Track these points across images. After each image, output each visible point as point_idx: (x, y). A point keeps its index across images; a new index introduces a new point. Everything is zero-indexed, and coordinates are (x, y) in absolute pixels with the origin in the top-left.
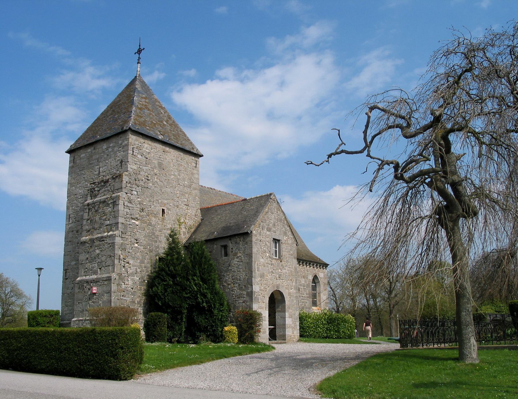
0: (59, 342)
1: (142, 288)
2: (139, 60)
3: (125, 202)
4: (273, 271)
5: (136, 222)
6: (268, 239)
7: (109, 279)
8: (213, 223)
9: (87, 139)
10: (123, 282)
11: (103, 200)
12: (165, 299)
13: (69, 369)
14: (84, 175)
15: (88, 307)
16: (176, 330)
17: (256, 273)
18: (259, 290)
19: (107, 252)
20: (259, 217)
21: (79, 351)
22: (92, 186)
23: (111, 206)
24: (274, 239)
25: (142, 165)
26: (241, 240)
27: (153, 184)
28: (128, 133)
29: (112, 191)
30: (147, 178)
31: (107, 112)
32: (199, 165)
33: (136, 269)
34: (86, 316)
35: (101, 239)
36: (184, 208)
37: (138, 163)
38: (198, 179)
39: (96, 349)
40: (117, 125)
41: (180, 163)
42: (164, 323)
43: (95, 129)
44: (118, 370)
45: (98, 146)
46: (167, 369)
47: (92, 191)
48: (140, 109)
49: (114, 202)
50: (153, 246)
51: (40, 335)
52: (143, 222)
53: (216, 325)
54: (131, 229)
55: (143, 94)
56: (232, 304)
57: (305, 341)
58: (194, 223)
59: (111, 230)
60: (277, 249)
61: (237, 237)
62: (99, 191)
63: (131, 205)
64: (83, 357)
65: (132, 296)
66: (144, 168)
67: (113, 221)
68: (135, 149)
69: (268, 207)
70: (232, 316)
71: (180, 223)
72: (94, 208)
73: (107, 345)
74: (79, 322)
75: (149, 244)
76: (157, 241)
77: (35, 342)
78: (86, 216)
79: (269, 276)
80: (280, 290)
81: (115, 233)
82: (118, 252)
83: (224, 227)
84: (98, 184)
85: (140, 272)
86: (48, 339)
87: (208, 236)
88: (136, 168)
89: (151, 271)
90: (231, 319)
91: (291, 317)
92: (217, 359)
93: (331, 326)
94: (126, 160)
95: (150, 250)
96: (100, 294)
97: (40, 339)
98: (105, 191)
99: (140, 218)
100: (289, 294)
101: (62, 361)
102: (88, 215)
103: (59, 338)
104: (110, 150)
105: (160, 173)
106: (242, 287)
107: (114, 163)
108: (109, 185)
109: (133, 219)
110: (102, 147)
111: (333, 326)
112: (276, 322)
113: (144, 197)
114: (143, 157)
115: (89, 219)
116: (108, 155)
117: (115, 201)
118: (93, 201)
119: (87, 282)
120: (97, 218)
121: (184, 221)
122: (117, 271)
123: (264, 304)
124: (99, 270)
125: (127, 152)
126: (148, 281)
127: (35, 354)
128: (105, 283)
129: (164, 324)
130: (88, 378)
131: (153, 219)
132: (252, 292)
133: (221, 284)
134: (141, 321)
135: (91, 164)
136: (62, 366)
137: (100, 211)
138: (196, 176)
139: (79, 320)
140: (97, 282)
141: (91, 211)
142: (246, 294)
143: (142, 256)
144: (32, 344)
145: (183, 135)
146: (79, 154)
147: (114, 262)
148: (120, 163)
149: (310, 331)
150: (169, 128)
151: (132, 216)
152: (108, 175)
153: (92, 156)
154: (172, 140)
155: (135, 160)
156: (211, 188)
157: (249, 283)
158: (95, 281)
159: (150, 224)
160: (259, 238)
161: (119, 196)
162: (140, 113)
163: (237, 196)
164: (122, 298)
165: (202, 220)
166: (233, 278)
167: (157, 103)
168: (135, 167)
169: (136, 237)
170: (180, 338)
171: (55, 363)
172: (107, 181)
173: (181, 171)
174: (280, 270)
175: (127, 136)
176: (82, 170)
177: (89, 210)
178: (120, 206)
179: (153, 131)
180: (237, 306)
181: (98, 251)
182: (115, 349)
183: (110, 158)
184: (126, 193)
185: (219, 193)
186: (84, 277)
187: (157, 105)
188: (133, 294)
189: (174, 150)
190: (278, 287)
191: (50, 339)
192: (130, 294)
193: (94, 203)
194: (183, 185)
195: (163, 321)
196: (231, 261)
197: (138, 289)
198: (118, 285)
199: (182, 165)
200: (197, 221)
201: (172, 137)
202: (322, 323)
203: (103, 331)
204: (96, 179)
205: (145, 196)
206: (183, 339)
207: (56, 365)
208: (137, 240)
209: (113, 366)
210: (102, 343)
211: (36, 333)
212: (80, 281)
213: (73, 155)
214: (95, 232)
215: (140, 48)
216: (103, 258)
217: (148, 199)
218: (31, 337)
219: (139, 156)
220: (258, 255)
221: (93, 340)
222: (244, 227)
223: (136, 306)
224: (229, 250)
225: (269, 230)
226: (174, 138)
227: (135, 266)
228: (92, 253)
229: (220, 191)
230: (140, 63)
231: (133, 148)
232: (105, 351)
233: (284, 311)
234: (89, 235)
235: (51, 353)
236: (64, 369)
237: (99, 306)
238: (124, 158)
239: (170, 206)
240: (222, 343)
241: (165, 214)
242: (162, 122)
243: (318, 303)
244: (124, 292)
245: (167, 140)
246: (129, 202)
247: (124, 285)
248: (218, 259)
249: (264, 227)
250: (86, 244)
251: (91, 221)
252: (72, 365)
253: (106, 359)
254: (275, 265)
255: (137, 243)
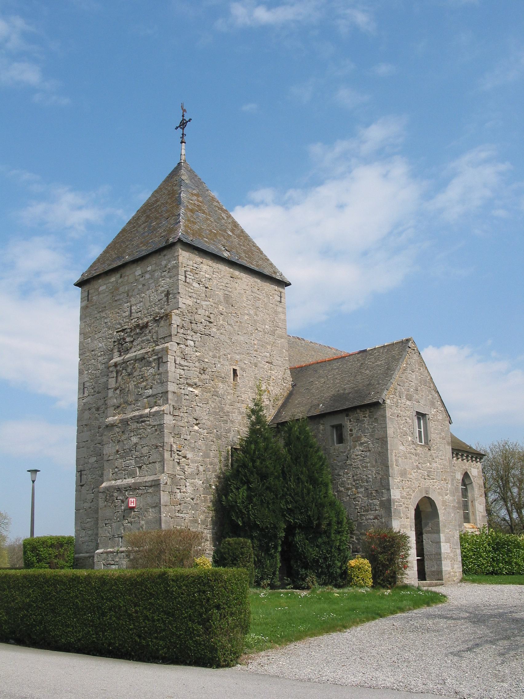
0: (98, 595)
1: (208, 498)
2: (182, 138)
3: (176, 358)
4: (419, 465)
5: (194, 390)
6: (408, 413)
7: (156, 484)
8: (314, 391)
9: (107, 262)
10: (179, 489)
11: (140, 356)
12: (249, 514)
13: (120, 645)
14: (106, 318)
15: (122, 531)
16: (266, 566)
17: (395, 470)
18: (399, 497)
19: (150, 439)
20: (394, 376)
21: (136, 612)
22: (120, 336)
23: (154, 365)
24: (418, 413)
25: (200, 298)
26: (367, 415)
27: (218, 330)
28: (176, 247)
29: (154, 341)
30: (207, 319)
31: (138, 219)
32: (285, 298)
33: (198, 467)
34: (118, 546)
35: (140, 419)
36: (266, 367)
37: (195, 296)
38: (284, 320)
39: (170, 608)
40: (156, 237)
41: (258, 296)
42: (250, 555)
43: (121, 246)
44: (213, 649)
45: (128, 271)
46: (291, 641)
47: (120, 342)
48: (192, 211)
49: (159, 358)
50: (222, 429)
51: (65, 584)
52: (205, 390)
53: (331, 557)
54: (187, 403)
55: (194, 189)
56: (355, 521)
57: (473, 581)
58: (281, 391)
59: (156, 404)
60: (422, 430)
61: (358, 411)
62: (132, 342)
63: (185, 363)
64: (146, 623)
65: (193, 512)
66: (204, 303)
67: (158, 389)
68: (188, 273)
69: (407, 362)
70: (356, 542)
71: (261, 391)
72: (126, 370)
73: (191, 602)
74: (107, 555)
75: (216, 425)
76: (227, 421)
77: (54, 596)
78: (112, 383)
79: (413, 474)
80: (430, 497)
81: (162, 408)
82: (169, 439)
83: (334, 395)
84: (131, 332)
85: (204, 471)
86: (78, 589)
87: (309, 411)
88: (191, 304)
89: (220, 469)
90: (355, 546)
91: (448, 541)
92: (368, 620)
93: (498, 555)
94: (175, 291)
95: (218, 435)
96: (141, 509)
97: (63, 589)
98: (143, 341)
99: (201, 384)
100: (444, 502)
101: (105, 631)
102: (116, 382)
103: (99, 588)
104: (147, 276)
105: (228, 311)
106: (372, 493)
107: (155, 297)
108: (150, 332)
109: (189, 385)
110: (135, 272)
111: (502, 554)
112: (425, 550)
113: (205, 350)
114: (201, 285)
115: (118, 388)
116: (144, 285)
117: (161, 358)
118: (123, 359)
119: (119, 489)
120: (132, 385)
121: (267, 387)
122: (168, 470)
123: (408, 520)
124: (138, 470)
125: (176, 277)
126: (216, 486)
127: (56, 617)
128: (148, 491)
129: (250, 558)
130: (156, 663)
131: (221, 385)
132: (389, 500)
133: (335, 488)
134: (208, 552)
135: (116, 301)
136: (106, 639)
137: (136, 374)
138: (282, 316)
139: (108, 553)
140: (136, 489)
141: (121, 374)
142: (380, 503)
143: (206, 445)
144: (50, 598)
145: (258, 252)
146: (96, 287)
147: (162, 456)
148: (165, 296)
149: (469, 562)
150: (236, 240)
151: (189, 381)
152: (146, 317)
153: (117, 289)
154: (244, 259)
155: (190, 290)
156: (298, 338)
157: (383, 486)
158: (133, 488)
159: (216, 394)
160: (395, 411)
161: (167, 348)
162: (192, 216)
163: (337, 350)
164: (177, 514)
165: (293, 386)
166: (355, 477)
167: (215, 204)
168: (189, 302)
169: (195, 415)
170: (272, 579)
171: (93, 634)
172: (146, 326)
173: (258, 308)
174: (428, 464)
175: (175, 252)
176: (102, 311)
177: (117, 374)
178: (169, 365)
179: (214, 244)
180: (364, 525)
181: (134, 440)
182: (206, 609)
183: (148, 290)
184: (178, 344)
185: (310, 345)
186: (113, 482)
187: (216, 206)
188: (195, 507)
189: (247, 276)
190: (427, 492)
191: (82, 591)
192: (190, 508)
193: (125, 362)
194: (262, 330)
195: (247, 552)
196: (349, 451)
197: (202, 500)
198: (171, 493)
199: (259, 299)
200: (285, 389)
201: (243, 255)
202: (485, 550)
203: (182, 576)
204: (127, 324)
205: (207, 349)
206: (278, 581)
207: (93, 638)
208: (197, 420)
209: (204, 641)
210: (182, 598)
211: (56, 580)
212: (107, 489)
213: (86, 288)
214: (129, 408)
215: (183, 120)
216: (145, 450)
217: (211, 354)
218: (48, 587)
219: (195, 285)
220: (395, 440)
221: (162, 593)
222: (370, 394)
223: (200, 528)
224: (346, 433)
225: (409, 398)
226: (246, 257)
227: (196, 462)
228: (125, 443)
229: (311, 342)
230: (185, 143)
231: (185, 271)
232: (187, 613)
233: (438, 532)
234: (119, 414)
235: (85, 614)
236: (110, 644)
237: (141, 529)
238: (172, 288)
239: (245, 364)
240: (350, 588)
241: (238, 378)
242: (225, 231)
243: (471, 517)
244: (180, 504)
245: (235, 259)
246: (182, 358)
247: (180, 494)
248: (327, 447)
249: (402, 393)
250: (115, 427)
251: (121, 390)
252: (124, 638)
253: (190, 628)
254: (421, 455)
255: (197, 424)
